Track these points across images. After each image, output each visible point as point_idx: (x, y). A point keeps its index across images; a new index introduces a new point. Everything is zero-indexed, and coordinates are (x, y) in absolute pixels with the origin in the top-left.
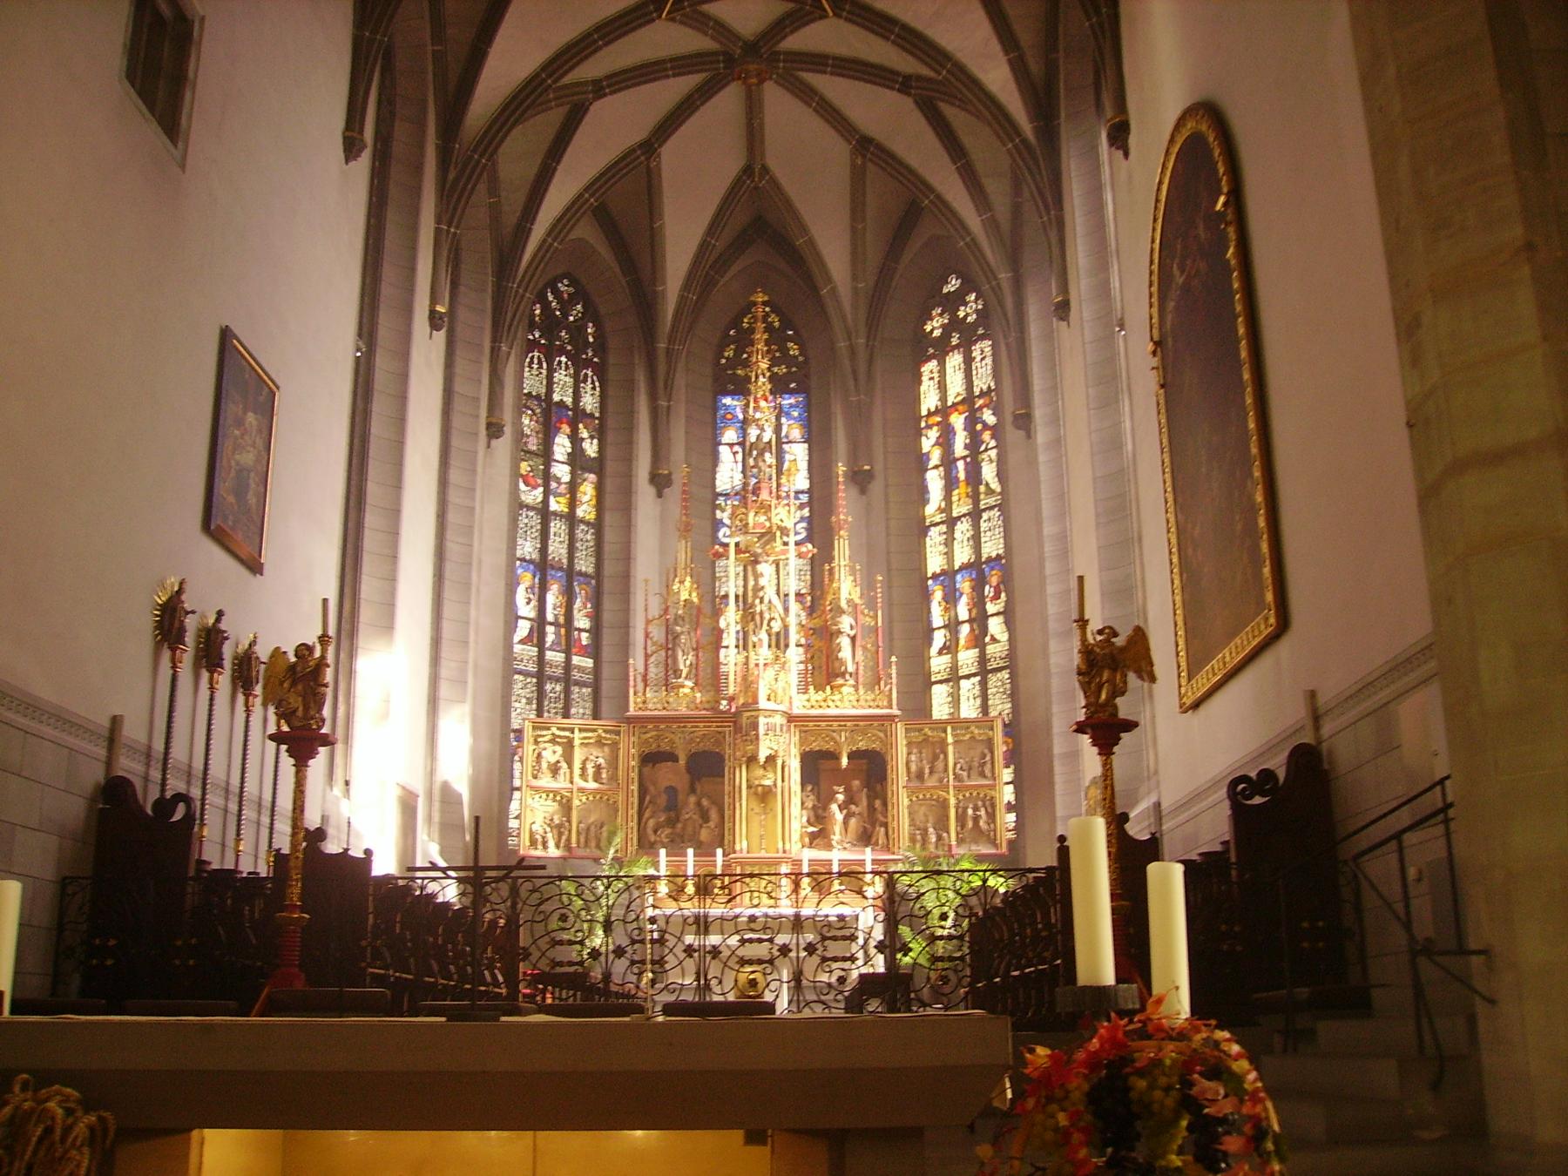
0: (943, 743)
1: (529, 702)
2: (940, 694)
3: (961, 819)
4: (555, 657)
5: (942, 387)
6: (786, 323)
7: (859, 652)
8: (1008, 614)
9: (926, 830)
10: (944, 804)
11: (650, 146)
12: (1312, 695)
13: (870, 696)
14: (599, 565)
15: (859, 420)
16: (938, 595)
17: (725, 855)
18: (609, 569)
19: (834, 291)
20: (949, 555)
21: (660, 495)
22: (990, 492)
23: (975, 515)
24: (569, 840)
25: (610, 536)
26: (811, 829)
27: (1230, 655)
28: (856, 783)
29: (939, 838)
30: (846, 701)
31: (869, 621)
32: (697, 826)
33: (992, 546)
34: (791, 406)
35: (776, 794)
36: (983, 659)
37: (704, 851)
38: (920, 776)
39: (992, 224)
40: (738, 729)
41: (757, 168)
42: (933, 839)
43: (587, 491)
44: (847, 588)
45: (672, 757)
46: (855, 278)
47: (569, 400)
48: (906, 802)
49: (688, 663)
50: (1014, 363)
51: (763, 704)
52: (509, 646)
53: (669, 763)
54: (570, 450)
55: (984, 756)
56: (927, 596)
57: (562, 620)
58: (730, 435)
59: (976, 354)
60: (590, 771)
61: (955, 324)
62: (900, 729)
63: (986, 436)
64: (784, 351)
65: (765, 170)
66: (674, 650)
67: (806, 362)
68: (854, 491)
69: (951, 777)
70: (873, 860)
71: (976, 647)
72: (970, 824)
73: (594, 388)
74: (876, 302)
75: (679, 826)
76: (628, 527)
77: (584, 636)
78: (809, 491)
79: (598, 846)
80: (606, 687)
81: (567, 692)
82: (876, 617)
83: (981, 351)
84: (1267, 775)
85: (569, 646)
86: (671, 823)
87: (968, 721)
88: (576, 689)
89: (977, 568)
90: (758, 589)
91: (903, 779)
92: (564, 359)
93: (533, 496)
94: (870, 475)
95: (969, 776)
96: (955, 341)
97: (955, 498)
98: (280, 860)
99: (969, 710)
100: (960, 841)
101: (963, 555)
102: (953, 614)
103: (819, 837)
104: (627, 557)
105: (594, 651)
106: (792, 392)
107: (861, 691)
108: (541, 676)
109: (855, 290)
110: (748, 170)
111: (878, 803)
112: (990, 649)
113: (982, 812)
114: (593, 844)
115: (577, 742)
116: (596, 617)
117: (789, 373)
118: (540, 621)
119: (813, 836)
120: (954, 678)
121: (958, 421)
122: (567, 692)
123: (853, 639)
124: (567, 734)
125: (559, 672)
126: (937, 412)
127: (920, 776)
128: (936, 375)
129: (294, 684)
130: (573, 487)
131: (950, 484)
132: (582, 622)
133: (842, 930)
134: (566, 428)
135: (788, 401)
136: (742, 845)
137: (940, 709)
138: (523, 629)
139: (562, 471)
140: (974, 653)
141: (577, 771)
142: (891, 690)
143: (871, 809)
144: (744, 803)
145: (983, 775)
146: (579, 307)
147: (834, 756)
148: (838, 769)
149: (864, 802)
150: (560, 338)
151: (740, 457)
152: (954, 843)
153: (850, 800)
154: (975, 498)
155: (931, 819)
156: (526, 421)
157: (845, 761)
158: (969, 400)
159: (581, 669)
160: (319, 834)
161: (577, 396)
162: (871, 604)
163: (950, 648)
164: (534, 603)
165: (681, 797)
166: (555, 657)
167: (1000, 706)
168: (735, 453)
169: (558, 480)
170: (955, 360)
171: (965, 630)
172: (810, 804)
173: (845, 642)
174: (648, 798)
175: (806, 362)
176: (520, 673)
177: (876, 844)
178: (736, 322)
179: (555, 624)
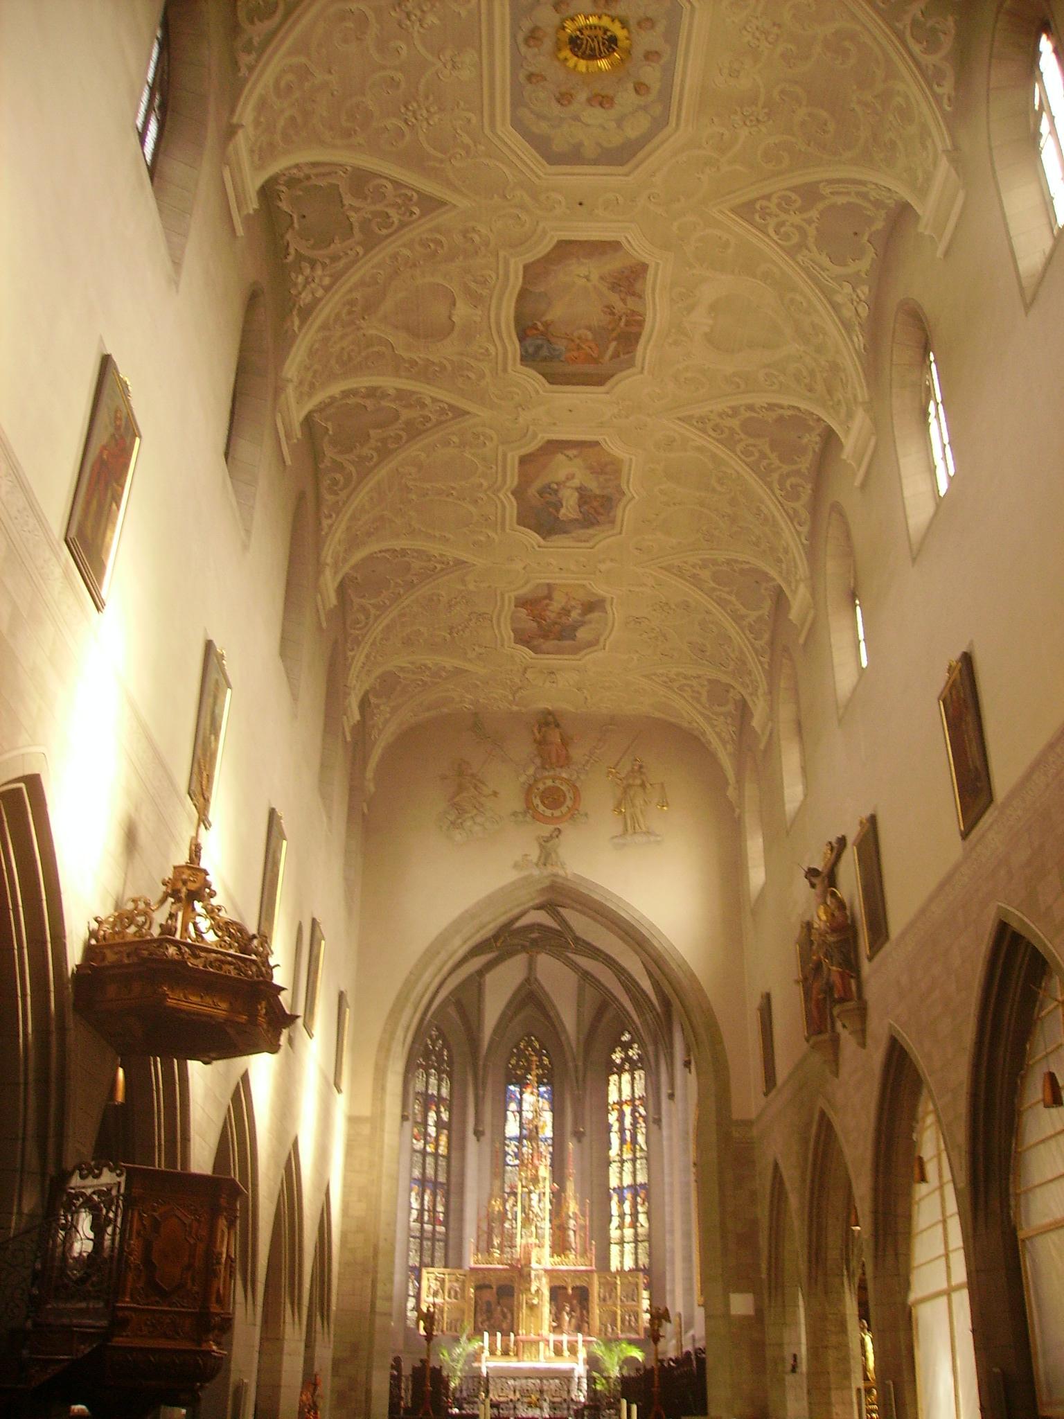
0: (616, 1283)
2: (615, 1249)
3: (623, 1321)
4: (428, 1227)
5: (620, 1090)
6: (542, 1046)
7: (578, 1237)
8: (648, 1213)
10: (615, 1313)
11: (481, 973)
14: (448, 1178)
15: (578, 1102)
16: (615, 1199)
17: (515, 1336)
18: (454, 1179)
19: (568, 1038)
20: (621, 1179)
21: (478, 1140)
22: (642, 1149)
23: (634, 1160)
24: (443, 1328)
25: (454, 1163)
26: (554, 1324)
28: (575, 1302)
29: (613, 1329)
30: (571, 1263)
31: (582, 1222)
33: (642, 1178)
34: (545, 1092)
36: (636, 1234)
37: (505, 1334)
39: (645, 1022)
40: (521, 1275)
41: (532, 979)
42: (610, 1330)
43: (443, 1140)
44: (572, 1207)
45: (490, 1287)
46: (578, 1032)
47: (435, 1093)
48: (598, 1311)
50: (653, 1085)
51: (534, 1265)
52: (409, 1221)
54: (436, 1119)
55: (633, 1290)
56: (610, 1198)
57: (431, 1208)
58: (513, 1106)
59: (636, 1076)
60: (453, 1293)
61: (627, 1059)
62: (595, 1276)
63: (641, 1120)
64: (541, 1060)
65: (536, 979)
67: (552, 1069)
68: (575, 1140)
70: (583, 1341)
72: (627, 1323)
73: (447, 1084)
74: (589, 1041)
75: (492, 1321)
76: (463, 1159)
77: (441, 1215)
78: (553, 1139)
79: (456, 1331)
80: (452, 1242)
81: (433, 1245)
82: (585, 1221)
83: (639, 1074)
85: (434, 1221)
86: (489, 1319)
89: (634, 1188)
90: (530, 1206)
92: (433, 1071)
93: (419, 1145)
94: (583, 1134)
96: (627, 1066)
97: (624, 1149)
100: (622, 1331)
101: (627, 1180)
103: (557, 1329)
104: (462, 1174)
105: (446, 1223)
106: (544, 1084)
108: (422, 1238)
109: (578, 1038)
110: (527, 980)
111: (585, 1312)
112: (640, 1230)
113: (633, 1318)
114: (453, 1329)
115: (447, 1280)
116: (447, 1206)
117: (544, 1074)
118: (421, 1211)
119: (555, 1328)
120: (621, 1242)
121: (627, 1109)
122: (433, 1245)
123: (575, 1231)
124: (442, 1276)
125: (430, 1235)
126: (618, 1103)
127: (604, 1300)
128: (617, 1083)
130: (437, 1139)
131: (623, 1141)
132: (440, 1208)
133: (566, 1377)
134: (434, 1108)
135: (543, 1089)
137: (614, 1265)
138: (414, 1214)
139: (432, 1130)
141: (446, 1294)
143: (582, 1315)
144: (524, 1310)
146: (441, 1042)
147: (565, 1288)
148: (566, 1294)
149: (578, 1311)
150: (431, 1060)
151: (518, 1118)
152: (619, 1332)
153: (572, 1310)
154: (634, 1151)
156: (416, 1107)
157: (570, 1291)
158: (633, 1100)
159: (440, 1233)
161: (439, 1090)
162: (584, 1215)
164: (419, 1201)
165: (493, 1306)
166: (428, 1227)
167: (643, 1260)
168: (515, 1116)
169: (430, 1136)
170: (626, 1077)
171: (628, 1219)
172: (553, 1312)
173: (571, 1233)
175: (552, 1069)
176: (413, 1237)
178: (517, 1046)
179: (429, 1211)
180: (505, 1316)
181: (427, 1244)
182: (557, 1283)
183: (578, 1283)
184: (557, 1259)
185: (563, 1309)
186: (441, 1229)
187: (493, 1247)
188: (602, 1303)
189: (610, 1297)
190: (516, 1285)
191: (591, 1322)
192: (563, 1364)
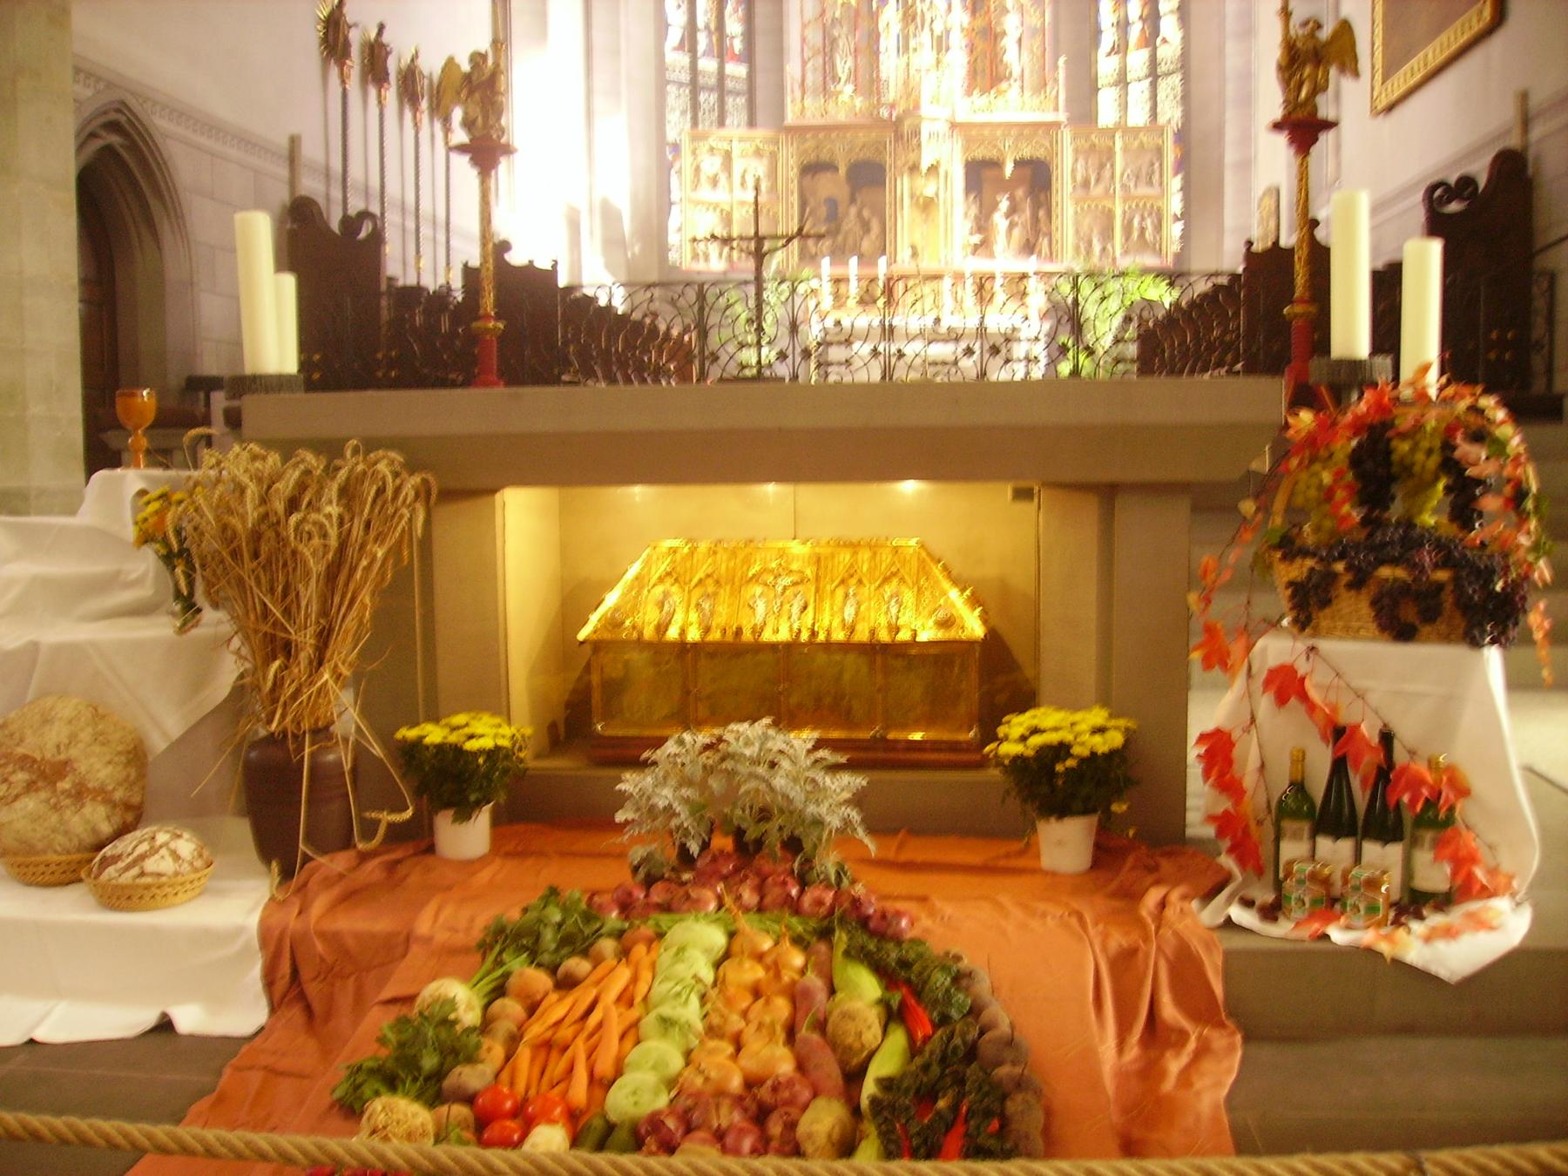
1: (683, 113)
2: (1107, 101)
4: (708, 65)
9: (1090, 243)
10: (1110, 215)
12: (1524, 97)
13: (1036, 101)
27: (1433, 54)
28: (1020, 193)
29: (1104, 249)
32: (858, 239)
35: (938, 205)
36: (1153, 62)
37: (867, 260)
38: (1086, 184)
40: (899, 137)
42: (1097, 247)
45: (831, 167)
49: (847, 67)
52: (660, 55)
53: (829, 175)
57: (713, 26)
62: (1067, 135)
66: (832, 58)
69: (1118, 186)
71: (1146, 46)
72: (1135, 235)
75: (840, 238)
84: (1467, 182)
85: (721, 52)
87: (1136, 131)
88: (730, 100)
91: (1068, 187)
95: (1136, 185)
98: (470, 273)
99: (1138, 116)
100: (1126, 252)
102: (1122, 14)
103: (983, 246)
107: (1027, 93)
108: (695, 87)
111: (1041, 213)
113: (1149, 223)
119: (976, 248)
125: (713, 81)
129: (471, 93)
132: (734, 27)
136: (904, 254)
137: (1107, 114)
138: (675, 35)
140: (1145, 53)
142: (1057, 97)
143: (1035, 219)
145: (1150, 183)
147: (996, 164)
149: (1028, 213)
153: (1013, 210)
155: (1095, 232)
157: (1009, 169)
160: (504, 246)
163: (1120, 48)
165: (841, 210)
166: (708, 65)
167: (1171, 113)
174: (808, 210)
177: (1040, 252)
180: (866, 227)
181: (708, 99)
182: (980, 153)
183: (1027, 152)
184: (979, 100)
185: (994, 207)
186: (736, 70)
187: (836, 79)
188: (1080, 192)
189: (1098, 180)
190: (889, 161)
191: (1057, 236)
192: (998, 321)
